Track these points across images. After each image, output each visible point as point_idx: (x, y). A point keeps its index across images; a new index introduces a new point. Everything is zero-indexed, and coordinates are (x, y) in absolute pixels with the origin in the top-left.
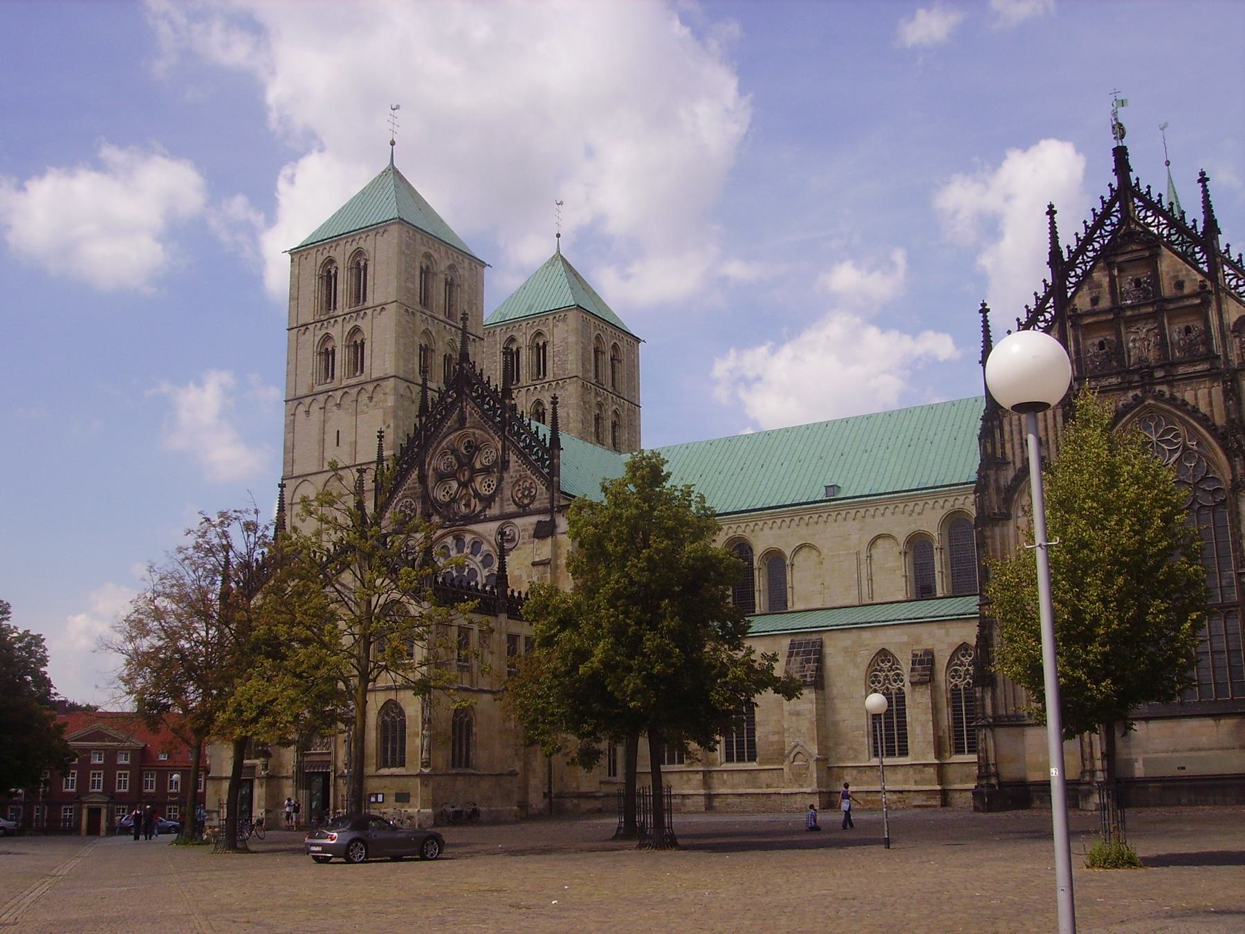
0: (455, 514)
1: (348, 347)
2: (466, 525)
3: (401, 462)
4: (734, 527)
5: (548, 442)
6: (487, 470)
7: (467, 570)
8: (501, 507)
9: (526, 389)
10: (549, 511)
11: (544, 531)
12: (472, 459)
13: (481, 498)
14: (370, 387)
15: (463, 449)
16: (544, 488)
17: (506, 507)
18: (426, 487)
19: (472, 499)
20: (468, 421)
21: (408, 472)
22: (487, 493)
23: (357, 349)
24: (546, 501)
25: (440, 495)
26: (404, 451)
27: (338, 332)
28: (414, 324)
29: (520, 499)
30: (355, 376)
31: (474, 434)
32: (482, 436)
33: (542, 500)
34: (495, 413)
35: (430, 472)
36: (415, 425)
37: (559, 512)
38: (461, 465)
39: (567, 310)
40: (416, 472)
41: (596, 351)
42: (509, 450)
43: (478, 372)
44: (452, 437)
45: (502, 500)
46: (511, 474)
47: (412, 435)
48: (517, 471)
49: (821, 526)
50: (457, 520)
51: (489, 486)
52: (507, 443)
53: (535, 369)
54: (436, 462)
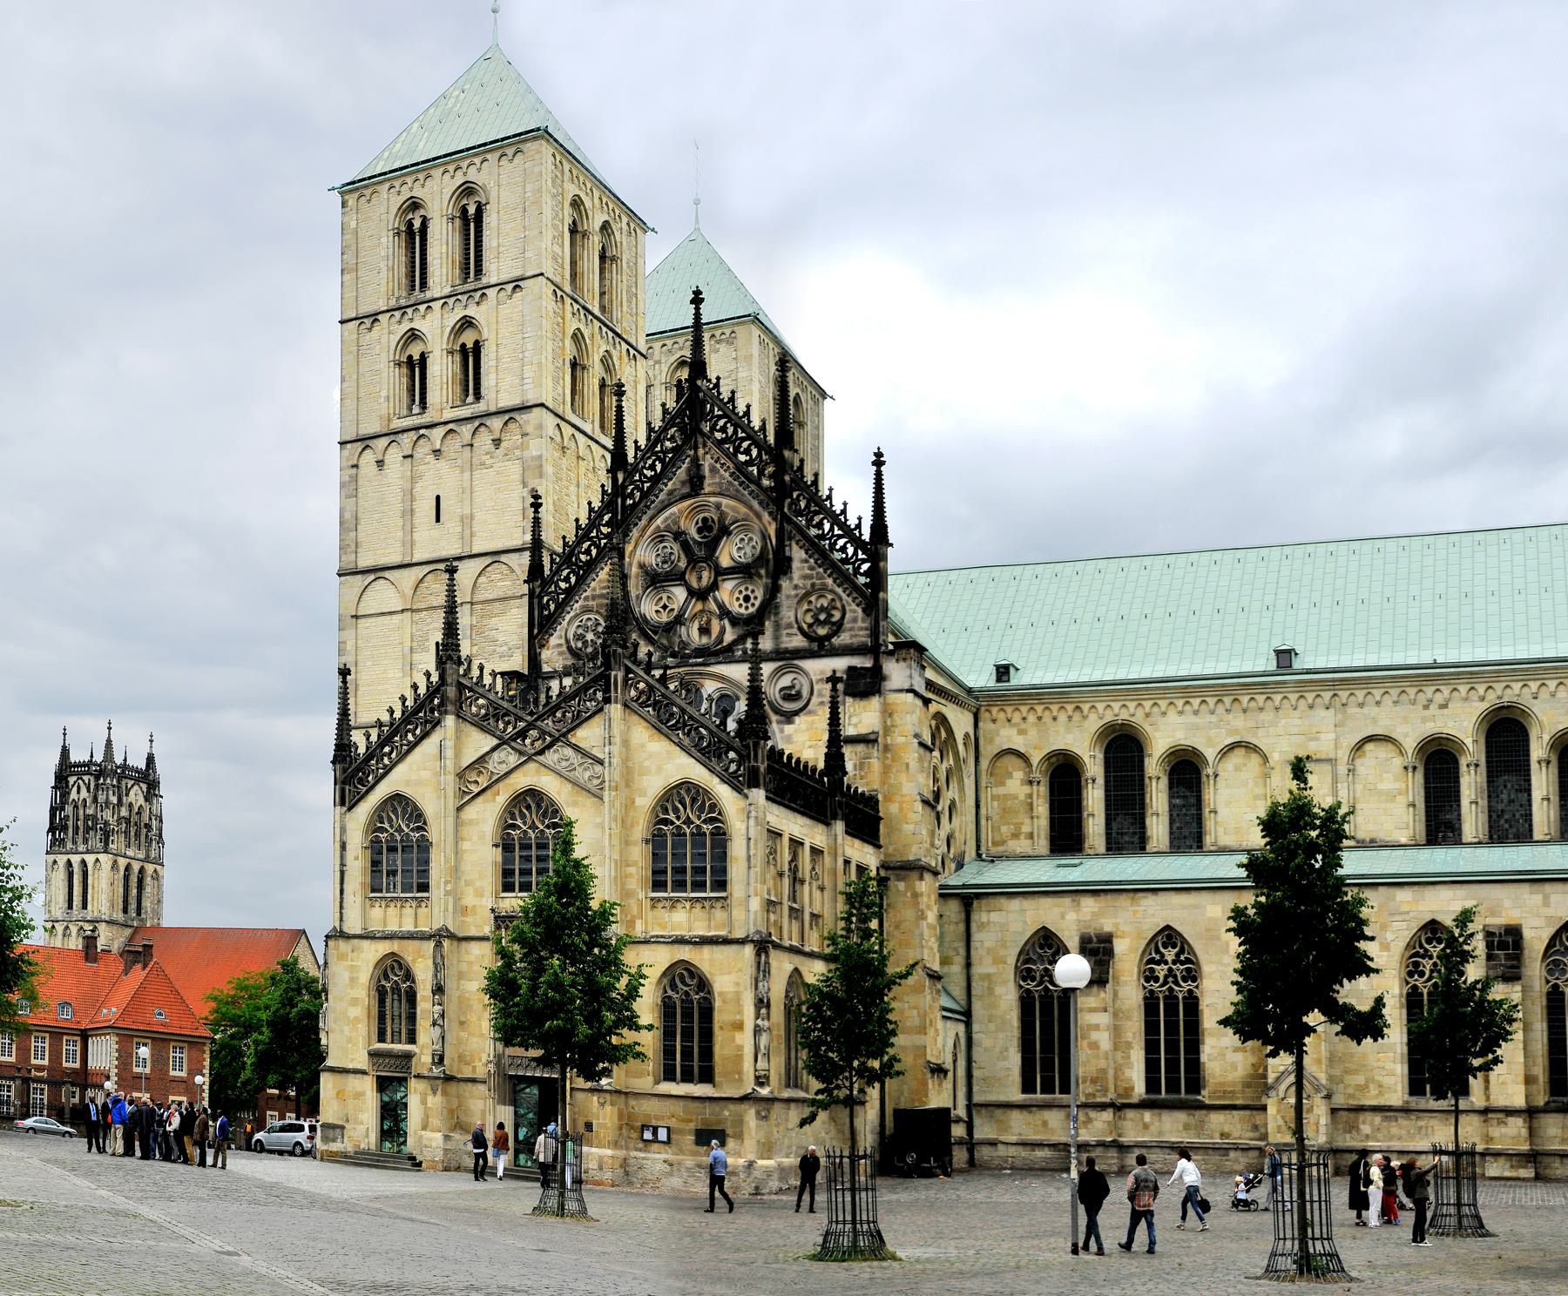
0: (684, 645)
1: (451, 352)
2: (708, 665)
4: (1116, 706)
6: (744, 571)
8: (776, 638)
10: (874, 649)
11: (865, 684)
13: (735, 621)
14: (496, 423)
15: (693, 532)
16: (859, 610)
17: (785, 639)
19: (715, 626)
21: (591, 566)
22: (742, 611)
23: (470, 358)
24: (861, 633)
25: (648, 608)
26: (583, 534)
27: (435, 327)
29: (810, 626)
30: (464, 403)
33: (855, 629)
35: (634, 570)
37: (891, 653)
38: (693, 561)
40: (607, 569)
42: (790, 539)
44: (674, 509)
45: (777, 627)
46: (796, 581)
47: (596, 504)
48: (805, 577)
49: (1267, 716)
50: (690, 657)
51: (747, 599)
52: (787, 527)
54: (642, 553)
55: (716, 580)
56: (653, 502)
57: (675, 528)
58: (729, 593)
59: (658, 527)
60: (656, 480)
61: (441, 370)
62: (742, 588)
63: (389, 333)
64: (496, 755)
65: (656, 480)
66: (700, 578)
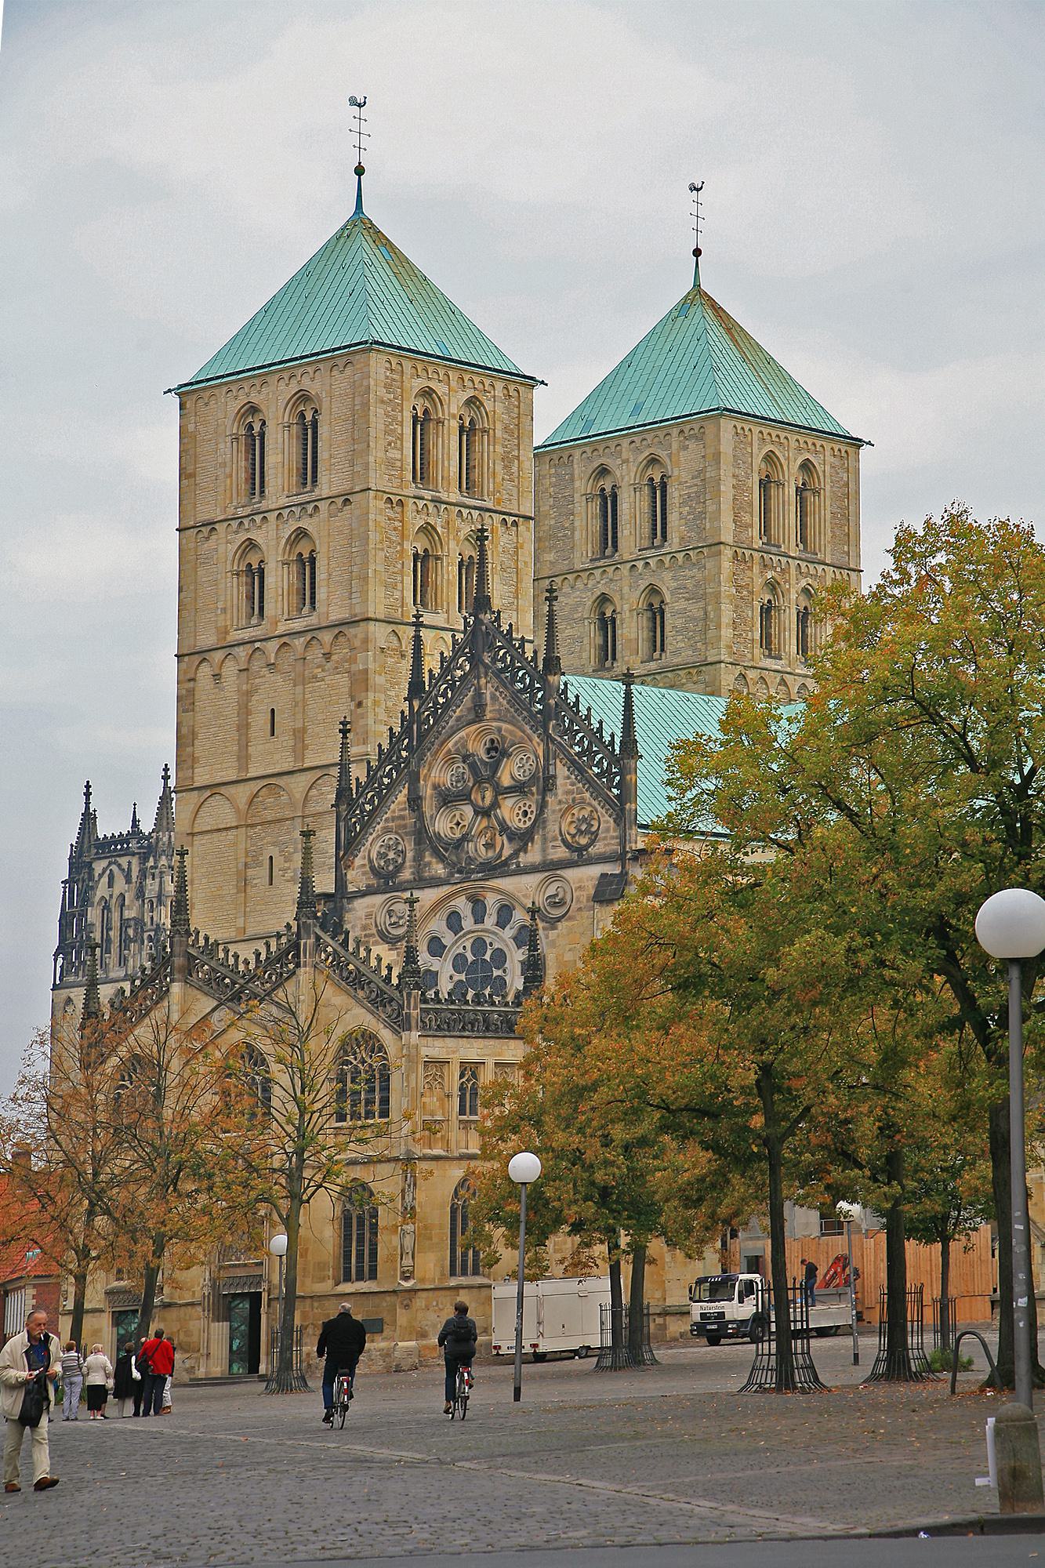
0: (470, 860)
2: (487, 880)
3: (380, 773)
5: (617, 748)
7: (489, 953)
9: (629, 565)
12: (495, 772)
18: (421, 817)
20: (489, 708)
28: (402, 521)
31: (499, 730)
32: (511, 732)
34: (533, 696)
36: (402, 712)
38: (479, 781)
39: (702, 419)
41: (765, 484)
43: (505, 628)
44: (462, 733)
50: (473, 871)
53: (646, 530)
55: (496, 798)
56: (444, 728)
57: (463, 752)
58: (511, 811)
59: (449, 750)
60: (446, 706)
61: (279, 580)
62: (521, 804)
63: (225, 546)
64: (216, 1014)
65: (446, 706)
66: (483, 798)
